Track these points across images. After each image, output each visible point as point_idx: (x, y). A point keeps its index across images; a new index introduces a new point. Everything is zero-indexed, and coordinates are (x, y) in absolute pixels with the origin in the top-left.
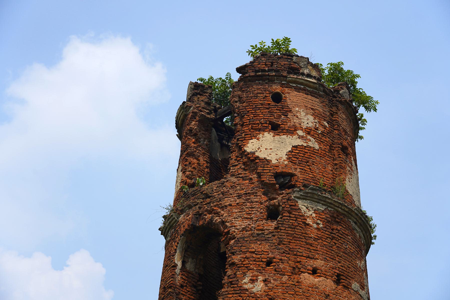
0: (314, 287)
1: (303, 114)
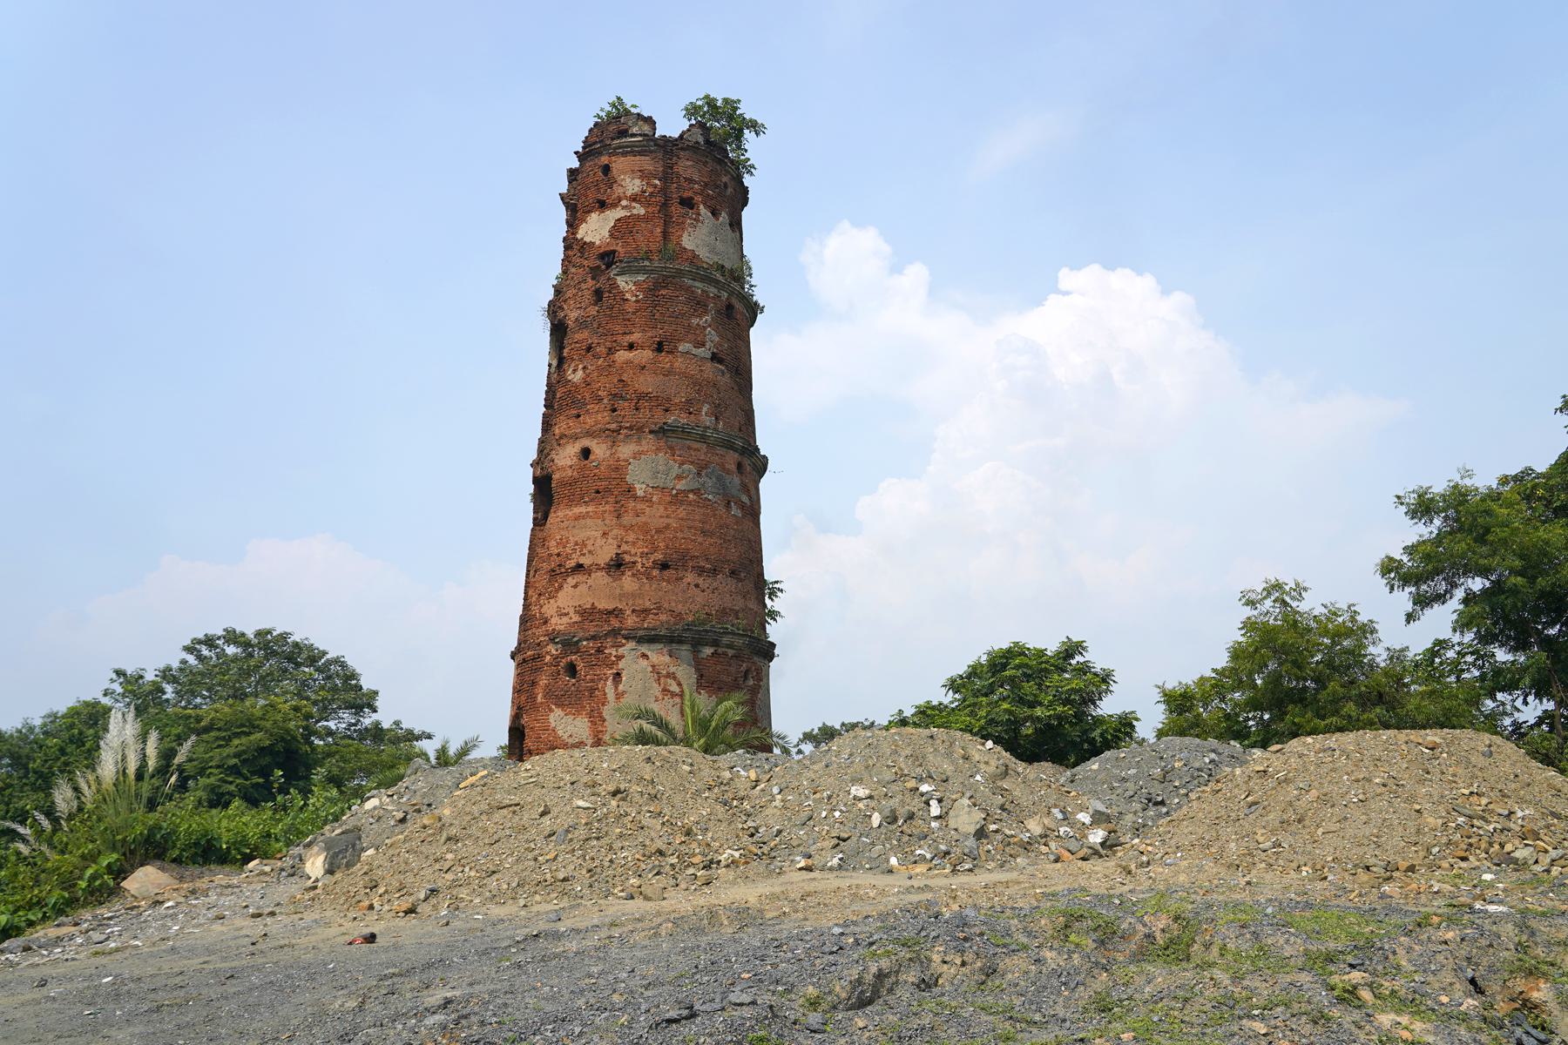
0: (628, 362)
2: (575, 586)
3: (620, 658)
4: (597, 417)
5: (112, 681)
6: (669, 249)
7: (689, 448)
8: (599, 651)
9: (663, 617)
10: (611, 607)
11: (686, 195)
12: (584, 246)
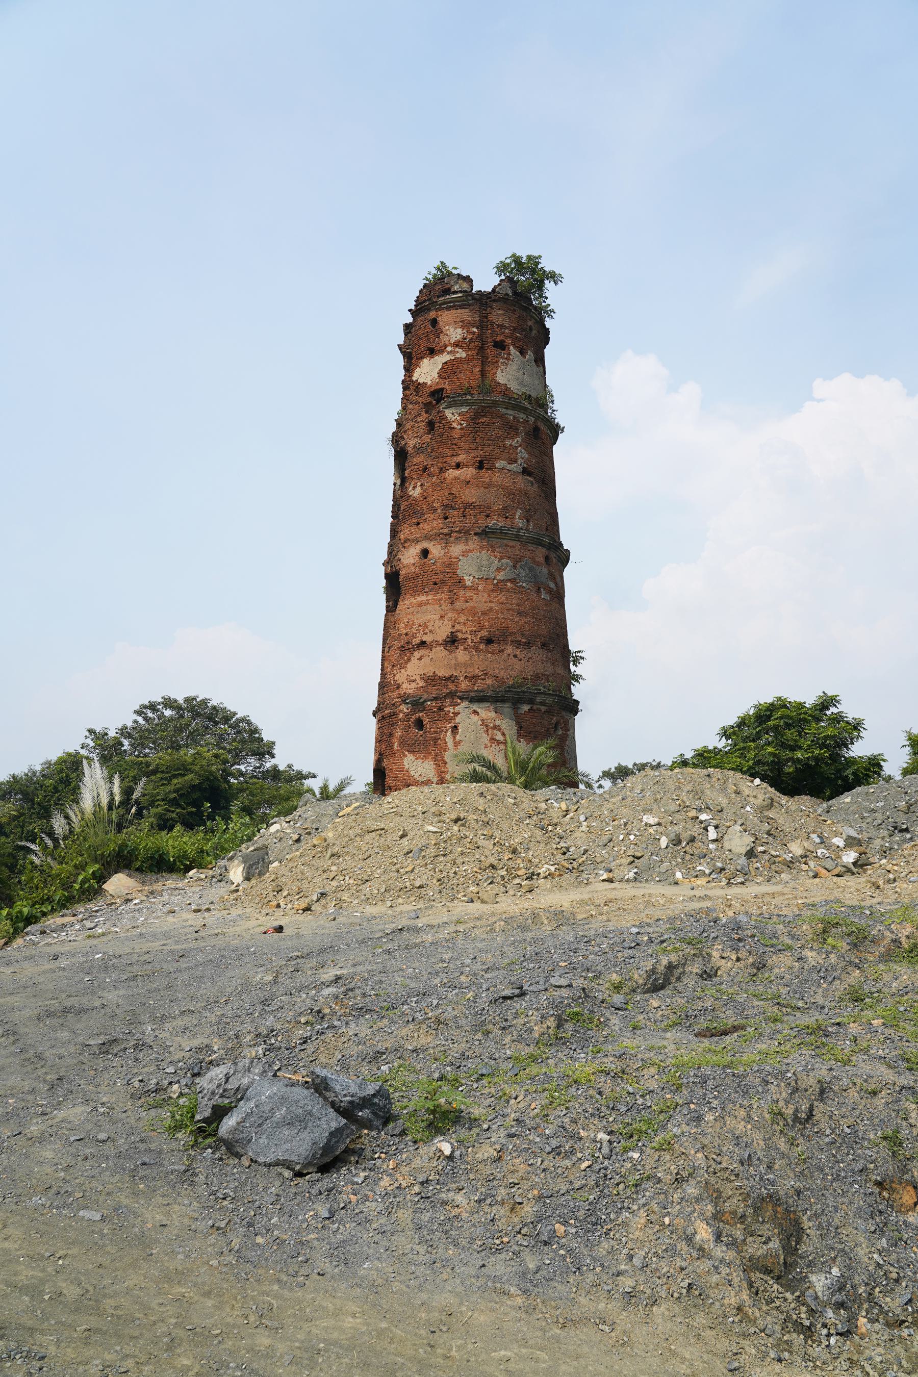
0: (456, 479)
1: (452, 330)
2: (420, 659)
3: (456, 714)
4: (433, 524)
5: (86, 737)
6: (486, 385)
7: (507, 546)
8: (441, 709)
9: (489, 682)
10: (448, 674)
11: (499, 338)
12: (419, 387)
